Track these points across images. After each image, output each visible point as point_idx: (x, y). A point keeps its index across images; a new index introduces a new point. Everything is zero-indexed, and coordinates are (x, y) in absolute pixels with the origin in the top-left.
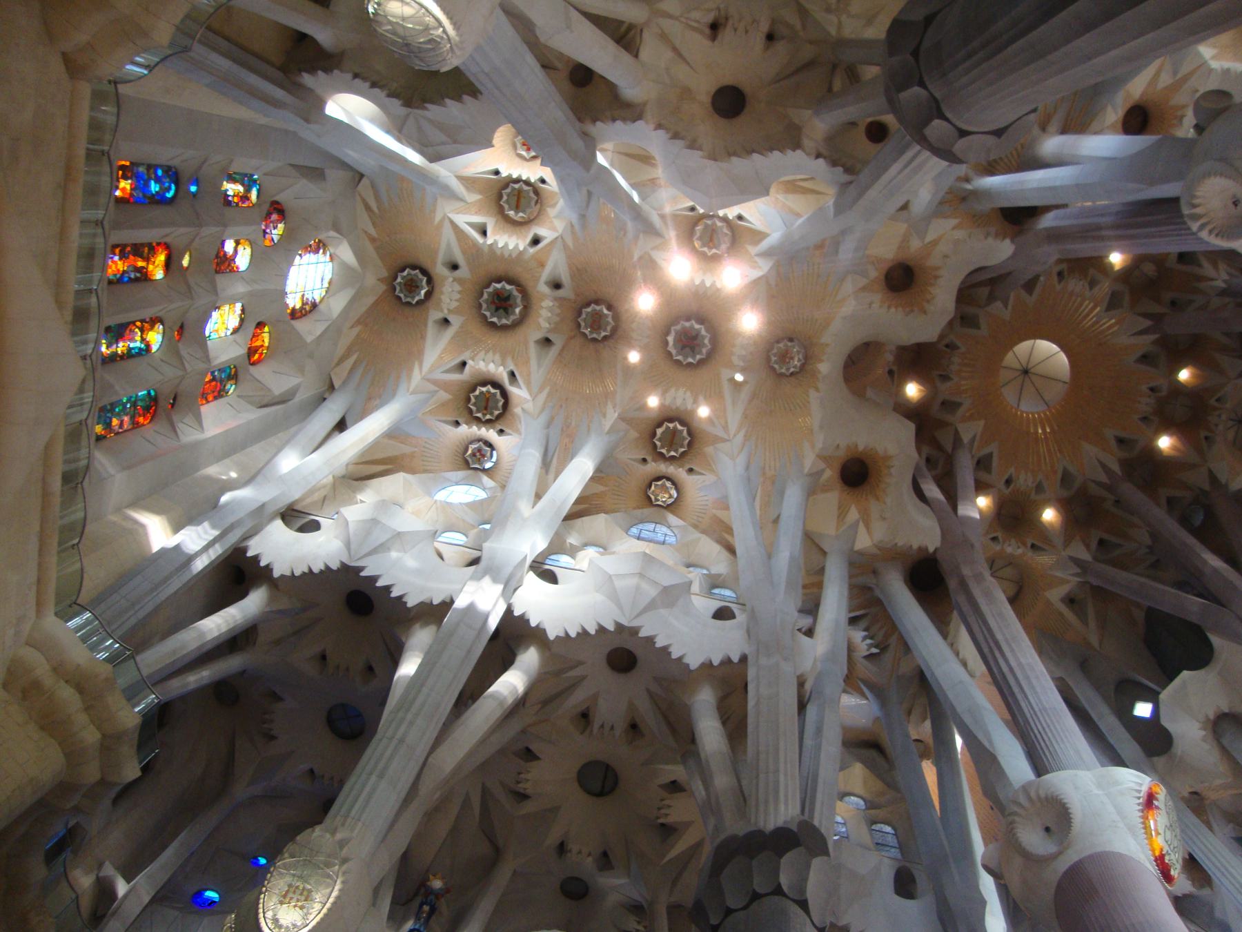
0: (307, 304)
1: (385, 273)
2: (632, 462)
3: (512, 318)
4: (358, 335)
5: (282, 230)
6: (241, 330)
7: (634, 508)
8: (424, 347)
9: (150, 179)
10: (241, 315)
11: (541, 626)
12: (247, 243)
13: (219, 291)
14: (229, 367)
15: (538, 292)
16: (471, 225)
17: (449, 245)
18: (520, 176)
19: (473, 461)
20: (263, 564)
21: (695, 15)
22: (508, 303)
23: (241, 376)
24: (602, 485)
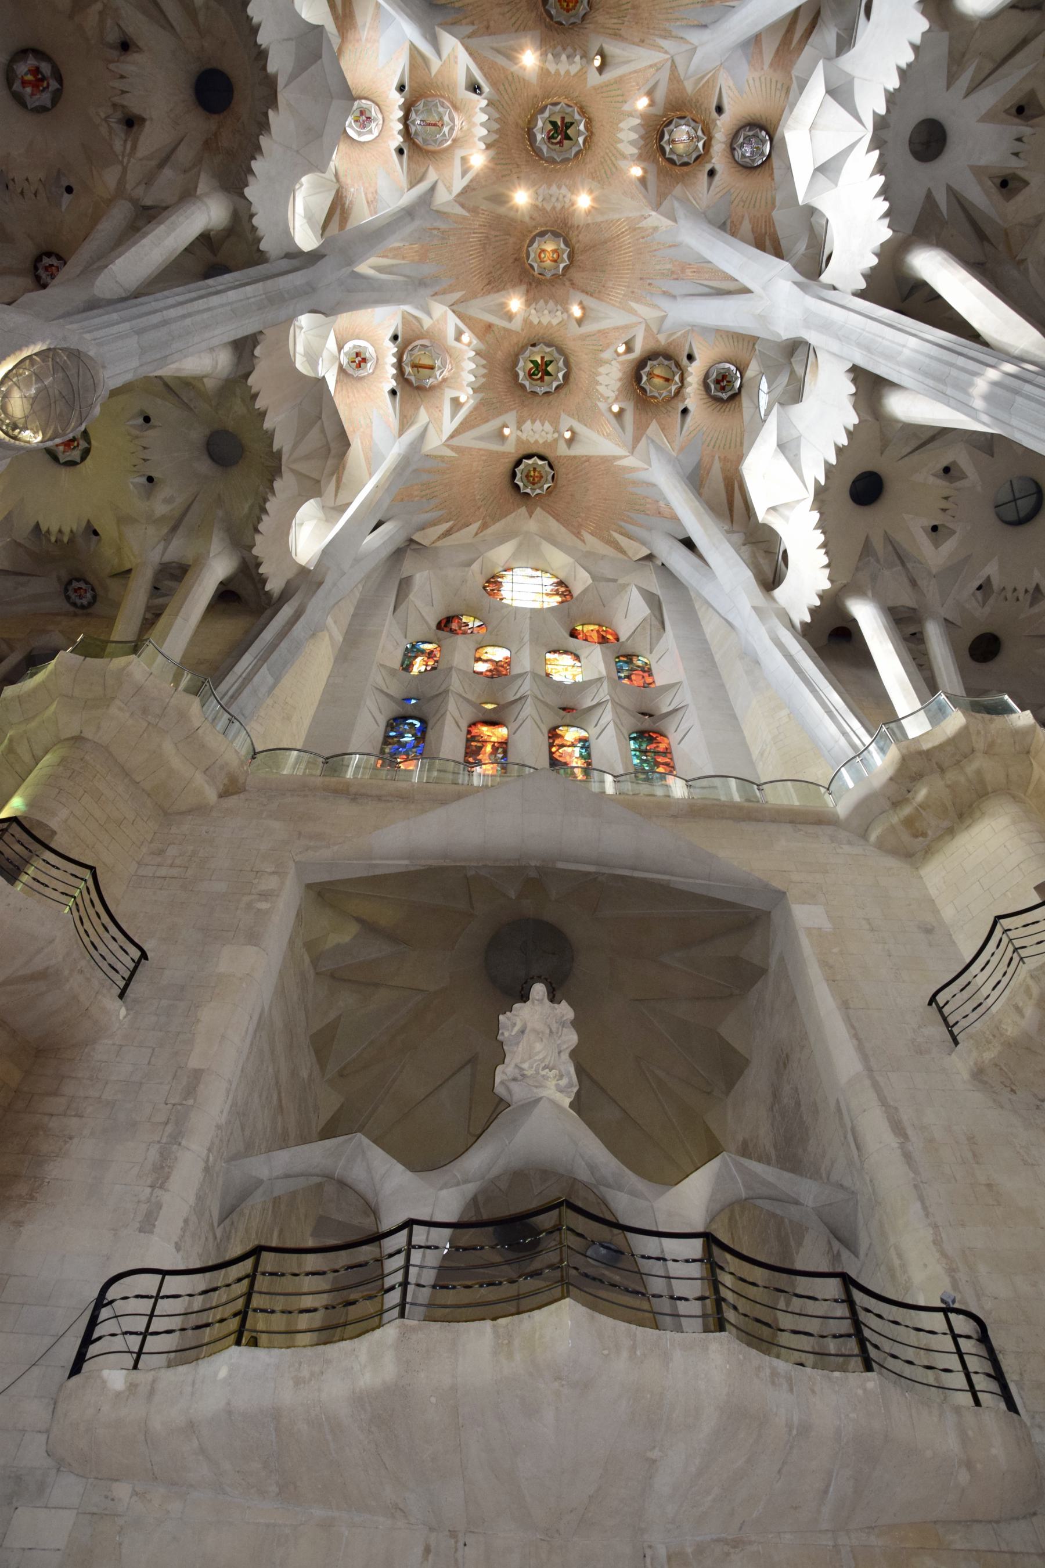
0: (557, 590)
2: (712, 188)
6: (577, 652)
7: (773, 179)
8: (598, 457)
9: (399, 741)
10: (560, 653)
11: (878, 250)
12: (480, 651)
14: (616, 662)
15: (523, 330)
16: (453, 417)
17: (481, 438)
18: (393, 365)
20: (818, 603)
21: (118, 145)
24: (741, 223)
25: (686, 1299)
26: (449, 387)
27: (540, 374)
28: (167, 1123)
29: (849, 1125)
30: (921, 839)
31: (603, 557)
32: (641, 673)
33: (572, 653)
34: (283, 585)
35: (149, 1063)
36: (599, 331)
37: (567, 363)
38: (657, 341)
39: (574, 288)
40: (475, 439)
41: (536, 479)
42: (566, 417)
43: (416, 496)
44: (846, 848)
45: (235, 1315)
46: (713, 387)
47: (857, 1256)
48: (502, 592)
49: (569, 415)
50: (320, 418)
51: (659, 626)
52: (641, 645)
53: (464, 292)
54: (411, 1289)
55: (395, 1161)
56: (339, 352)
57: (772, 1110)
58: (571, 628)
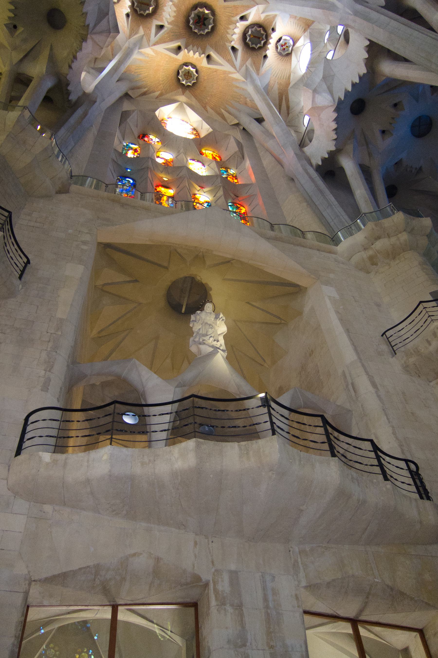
0: (192, 132)
1: (180, 90)
3: (211, 16)
6: (203, 163)
13: (182, 166)
16: (156, 35)
17: (168, 49)
19: (287, 51)
20: (327, 156)
22: (201, 16)
28: (49, 341)
29: (350, 381)
30: (374, 266)
31: (216, 120)
32: (232, 177)
33: (200, 162)
34: (76, 98)
35: (36, 313)
36: (234, 6)
37: (214, 21)
38: (260, 18)
42: (209, 47)
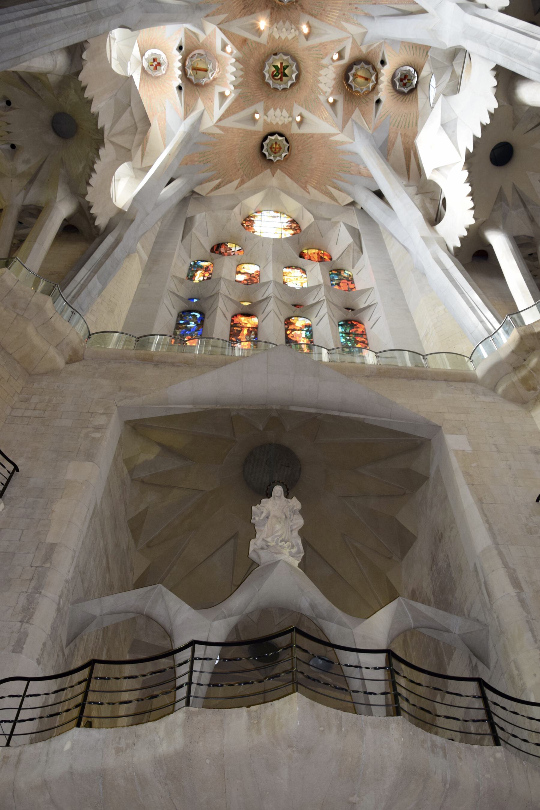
0: (291, 226)
4: (315, 188)
5: (232, 244)
6: (304, 268)
8: (318, 134)
9: (186, 327)
10: (292, 268)
12: (240, 266)
14: (330, 275)
15: (268, 43)
16: (220, 106)
17: (239, 121)
18: (179, 68)
19: (410, 86)
20: (465, 233)
23: (339, 267)
25: (375, 694)
26: (217, 84)
27: (280, 75)
29: (483, 581)
30: (532, 392)
31: (322, 203)
32: (346, 281)
33: (300, 268)
35: (20, 540)
36: (321, 44)
37: (298, 68)
38: (361, 51)
39: (303, 12)
40: (235, 121)
41: (277, 150)
42: (298, 106)
43: (196, 161)
44: (482, 398)
45: (76, 706)
46: (398, 84)
47: (488, 667)
48: (254, 227)
49: (299, 105)
50: (130, 105)
51: (359, 250)
52: (346, 263)
53: (227, 15)
54: (193, 687)
55: (184, 603)
56: (142, 58)
57: (432, 570)
58: (301, 251)
